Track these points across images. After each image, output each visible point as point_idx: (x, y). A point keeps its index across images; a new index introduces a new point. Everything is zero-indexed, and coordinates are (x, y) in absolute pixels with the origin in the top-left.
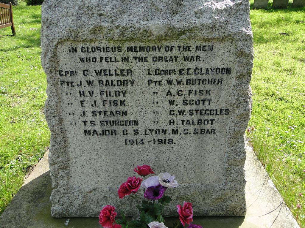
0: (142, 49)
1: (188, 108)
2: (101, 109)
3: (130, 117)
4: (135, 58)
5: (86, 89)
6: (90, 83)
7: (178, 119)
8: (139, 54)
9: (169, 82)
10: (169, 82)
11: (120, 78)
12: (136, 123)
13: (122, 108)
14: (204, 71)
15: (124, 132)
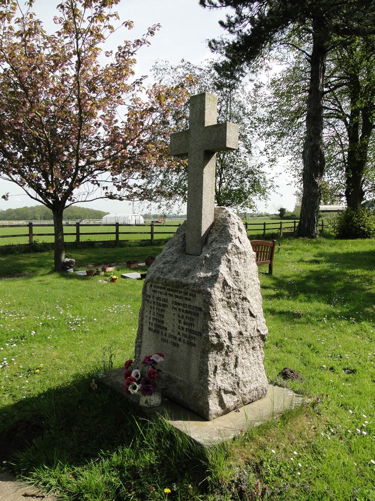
0: (172, 290)
1: (185, 327)
2: (155, 317)
3: (165, 325)
4: (169, 294)
5: (152, 305)
6: (154, 303)
7: (181, 332)
8: (171, 293)
9: (180, 310)
10: (180, 310)
11: (163, 303)
12: (166, 329)
13: (162, 319)
14: (192, 307)
15: (162, 332)
